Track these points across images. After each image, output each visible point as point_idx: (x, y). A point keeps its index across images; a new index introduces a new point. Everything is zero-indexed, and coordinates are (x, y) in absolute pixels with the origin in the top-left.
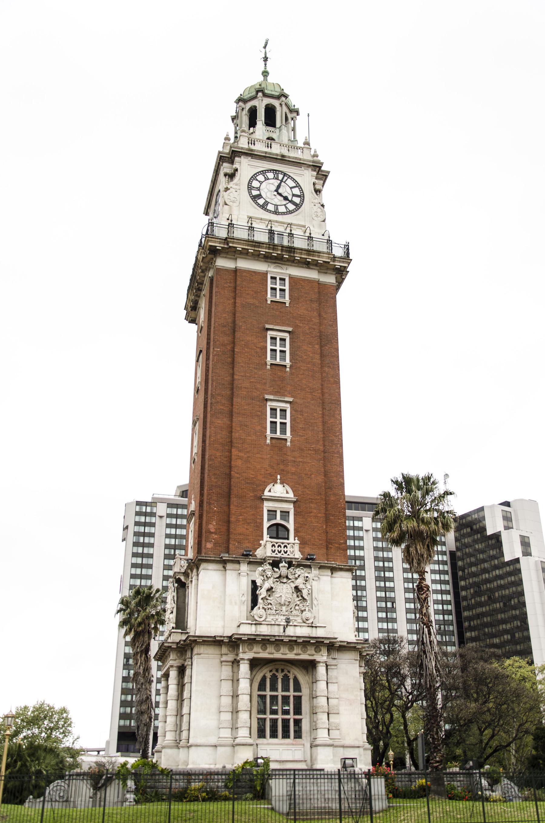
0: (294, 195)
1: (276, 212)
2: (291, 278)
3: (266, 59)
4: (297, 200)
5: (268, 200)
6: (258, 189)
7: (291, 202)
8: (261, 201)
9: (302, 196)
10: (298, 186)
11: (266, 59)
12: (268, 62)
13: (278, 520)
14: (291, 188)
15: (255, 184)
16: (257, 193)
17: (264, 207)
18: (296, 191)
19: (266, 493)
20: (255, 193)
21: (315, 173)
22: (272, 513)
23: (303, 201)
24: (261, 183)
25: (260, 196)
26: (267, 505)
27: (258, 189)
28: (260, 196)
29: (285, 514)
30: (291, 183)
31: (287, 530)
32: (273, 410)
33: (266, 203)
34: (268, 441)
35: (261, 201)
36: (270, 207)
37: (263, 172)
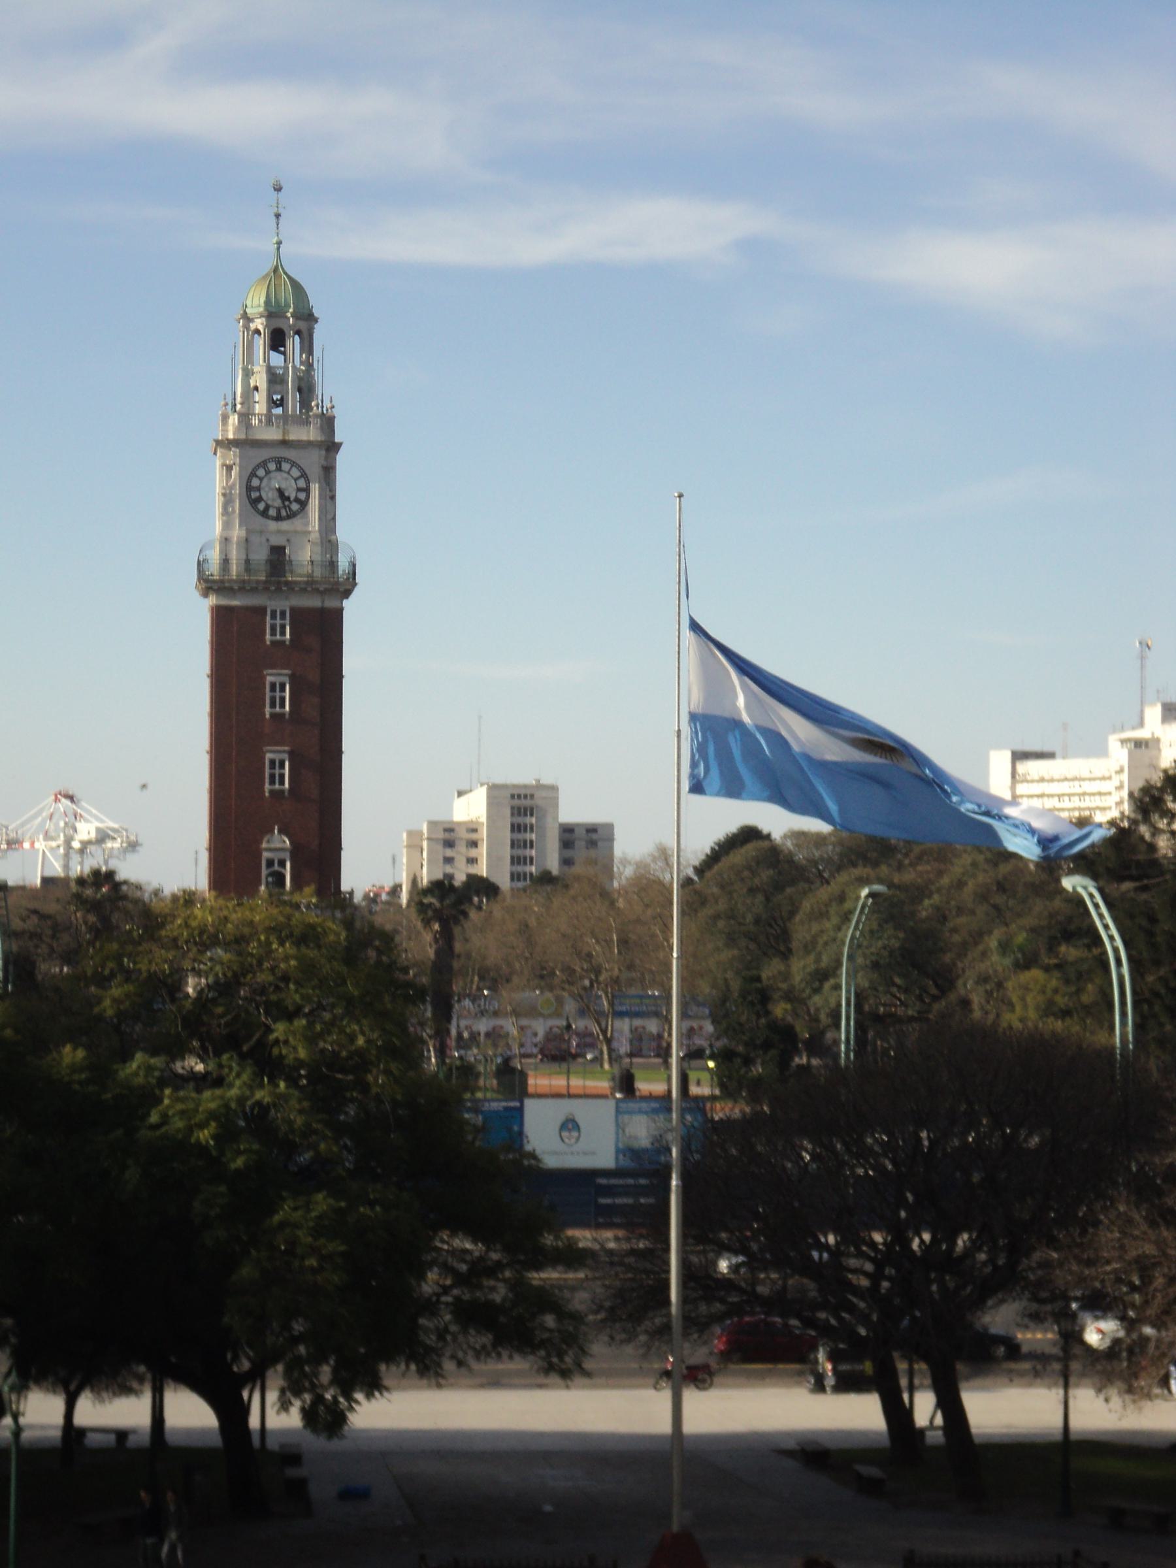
0: (299, 490)
1: (278, 518)
2: (292, 609)
3: (278, 216)
4: (302, 496)
5: (270, 502)
6: (258, 489)
7: (297, 500)
8: (261, 506)
9: (307, 490)
10: (304, 475)
11: (278, 216)
12: (281, 219)
13: (276, 867)
14: (296, 480)
15: (255, 482)
16: (257, 494)
17: (264, 514)
18: (302, 483)
19: (264, 845)
20: (254, 495)
21: (323, 452)
22: (270, 863)
23: (308, 497)
24: (261, 479)
25: (260, 499)
26: (266, 855)
27: (258, 489)
28: (260, 499)
29: (282, 863)
30: (295, 473)
31: (283, 877)
32: (272, 762)
33: (267, 507)
34: (267, 794)
35: (261, 506)
36: (272, 512)
37: (264, 464)
